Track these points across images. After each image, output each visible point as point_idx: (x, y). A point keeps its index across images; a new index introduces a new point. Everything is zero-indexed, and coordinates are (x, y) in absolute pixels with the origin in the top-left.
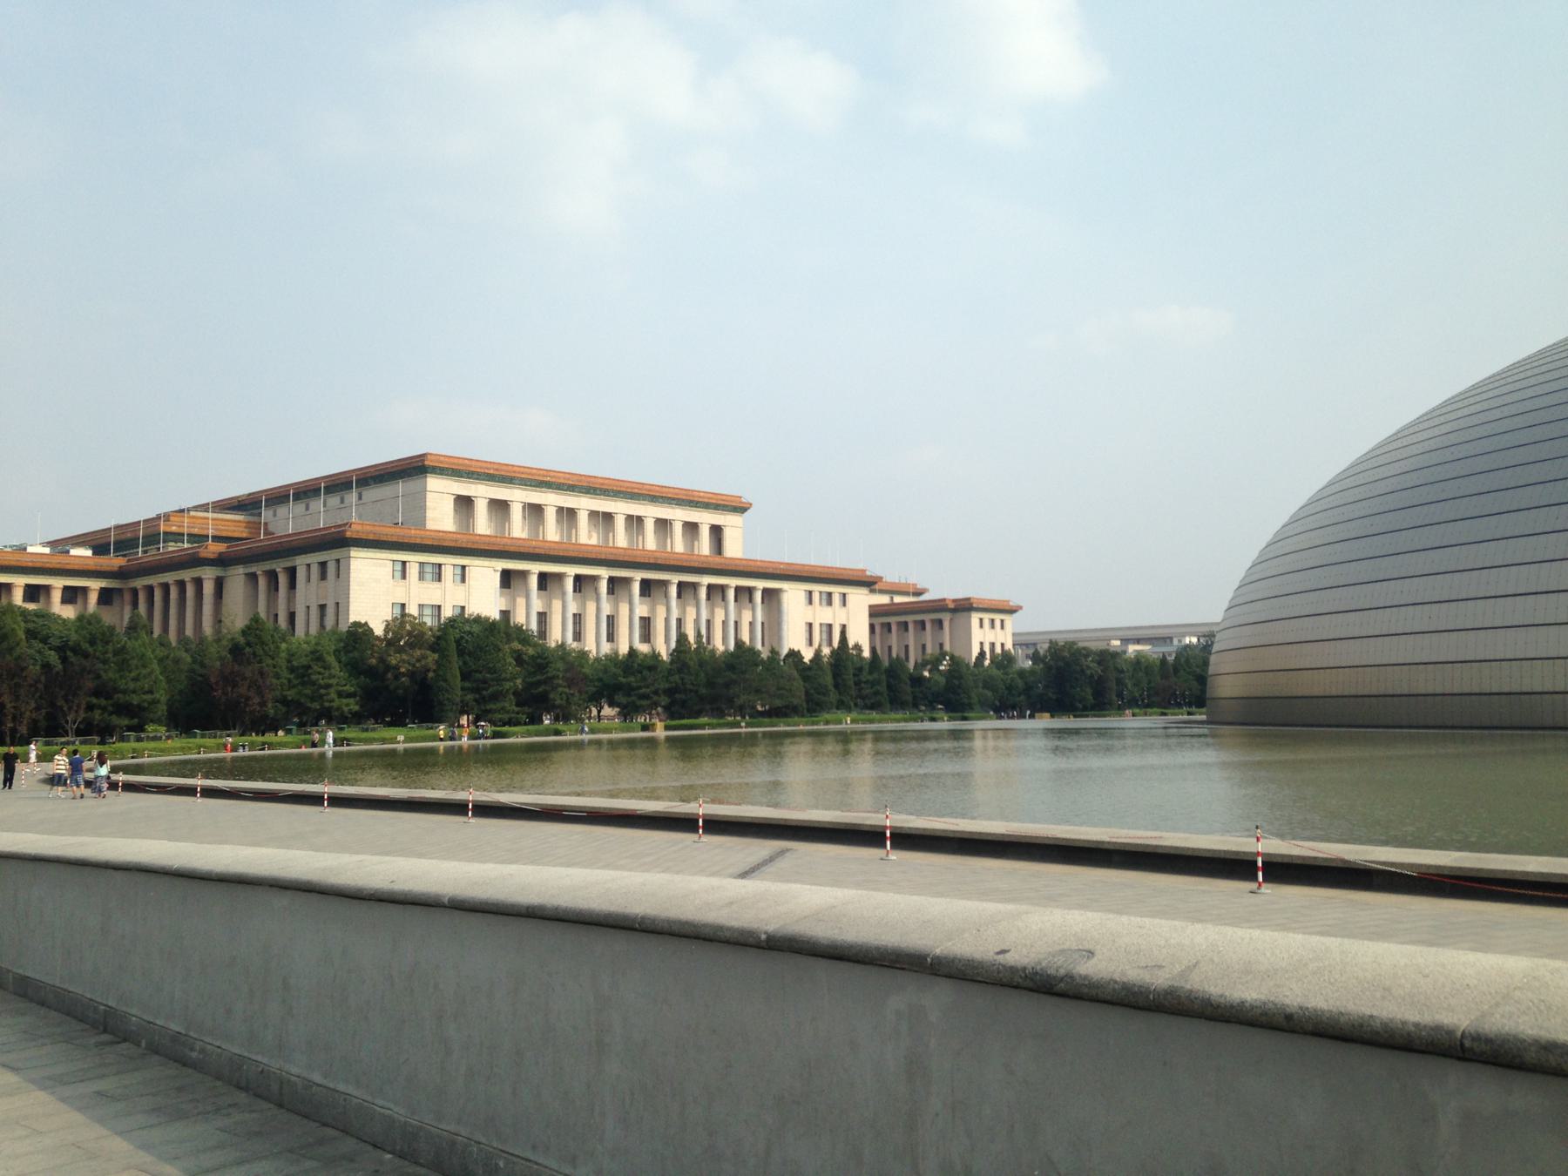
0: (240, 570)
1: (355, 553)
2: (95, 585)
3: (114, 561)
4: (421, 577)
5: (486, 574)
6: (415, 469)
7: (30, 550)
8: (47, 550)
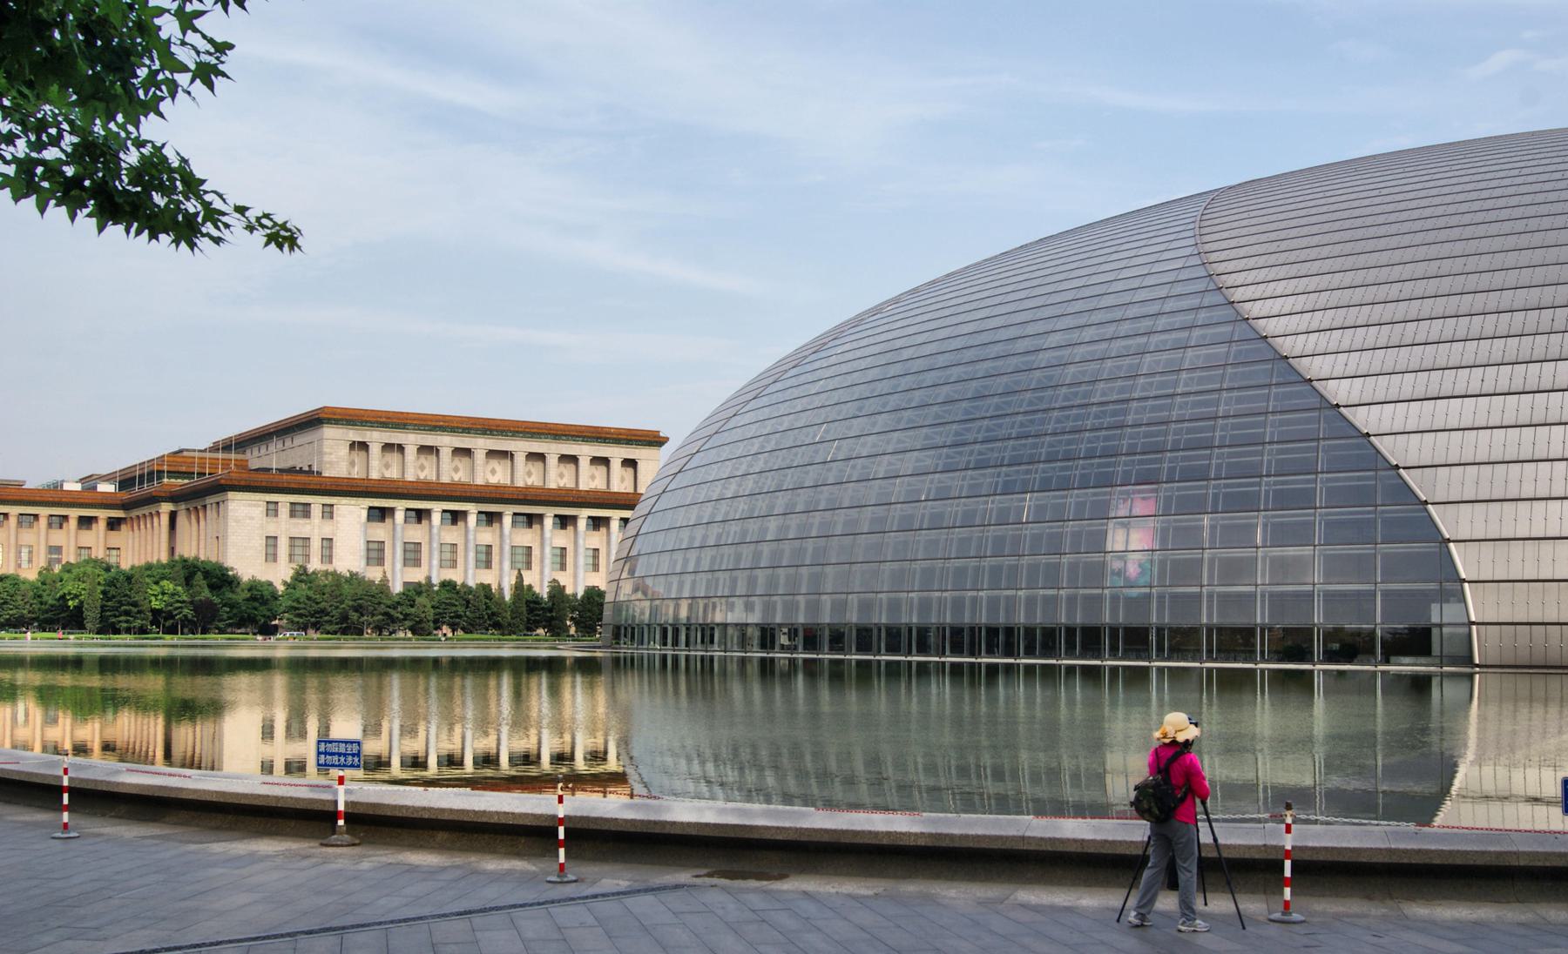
0: (183, 506)
1: (231, 495)
2: (103, 514)
3: (125, 496)
4: (293, 514)
5: (352, 512)
6: (312, 422)
7: (67, 487)
8: (78, 487)
